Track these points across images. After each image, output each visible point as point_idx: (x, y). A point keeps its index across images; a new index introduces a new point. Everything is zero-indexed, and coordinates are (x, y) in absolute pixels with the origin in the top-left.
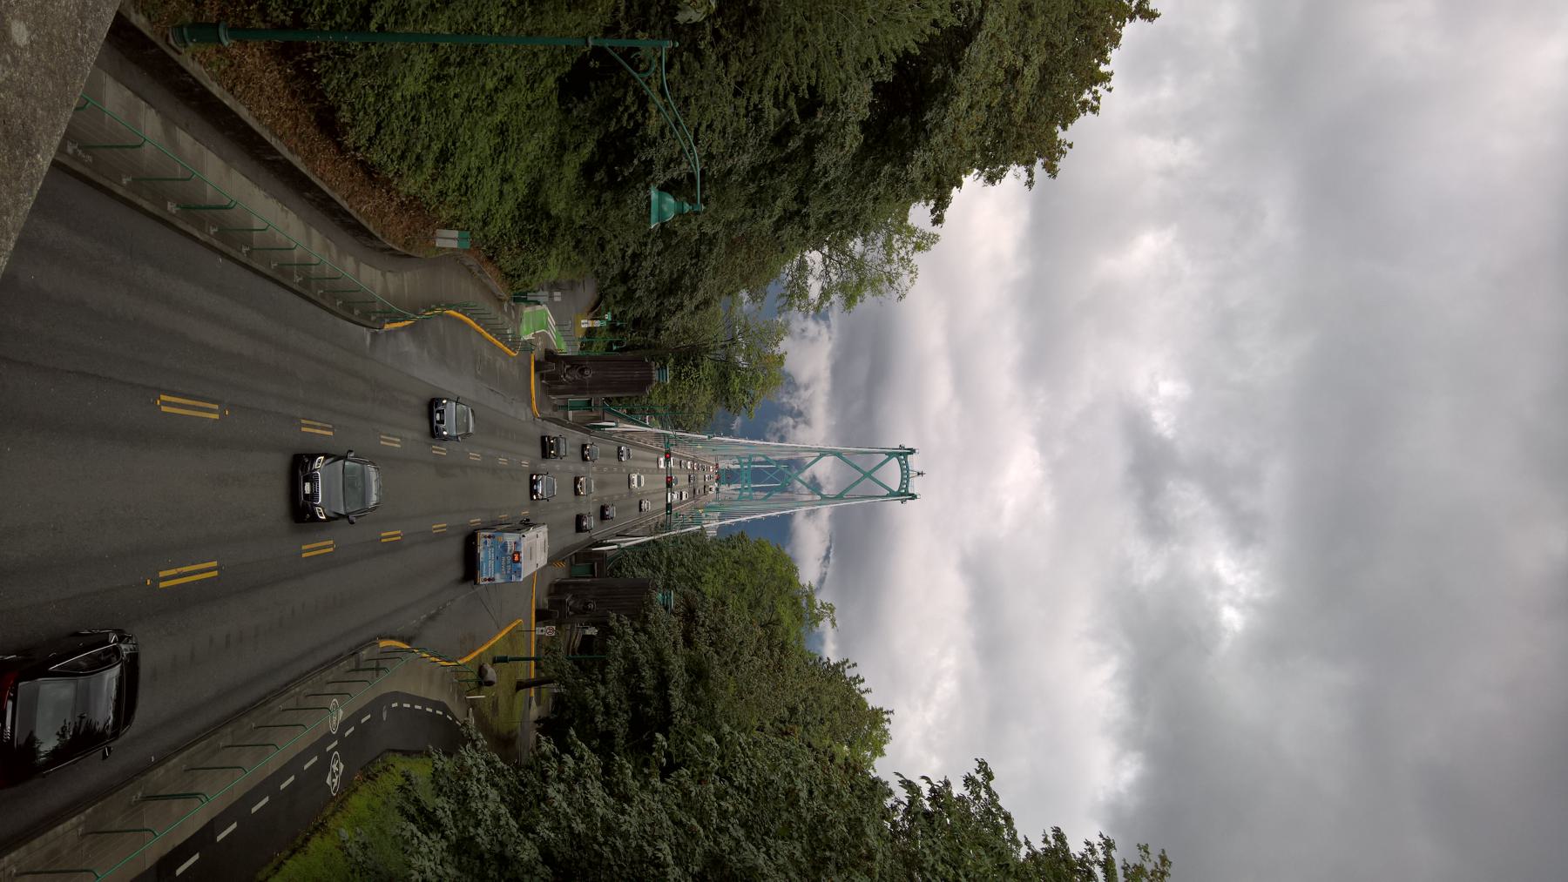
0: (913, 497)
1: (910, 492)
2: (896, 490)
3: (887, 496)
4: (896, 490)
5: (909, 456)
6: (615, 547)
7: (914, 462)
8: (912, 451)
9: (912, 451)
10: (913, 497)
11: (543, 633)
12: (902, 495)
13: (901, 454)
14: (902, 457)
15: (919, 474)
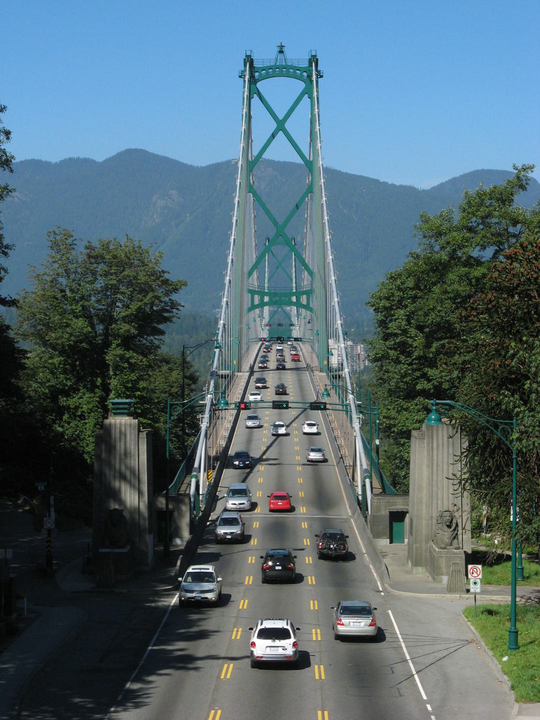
0: (314, 60)
1: (306, 64)
2: (301, 86)
3: (311, 97)
4: (301, 86)
5: (256, 65)
6: (368, 481)
7: (265, 56)
8: (249, 60)
9: (249, 60)
10: (314, 60)
11: (479, 581)
12: (310, 77)
13: (252, 76)
14: (257, 74)
15: (281, 52)
